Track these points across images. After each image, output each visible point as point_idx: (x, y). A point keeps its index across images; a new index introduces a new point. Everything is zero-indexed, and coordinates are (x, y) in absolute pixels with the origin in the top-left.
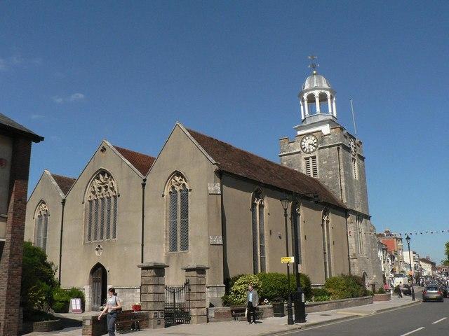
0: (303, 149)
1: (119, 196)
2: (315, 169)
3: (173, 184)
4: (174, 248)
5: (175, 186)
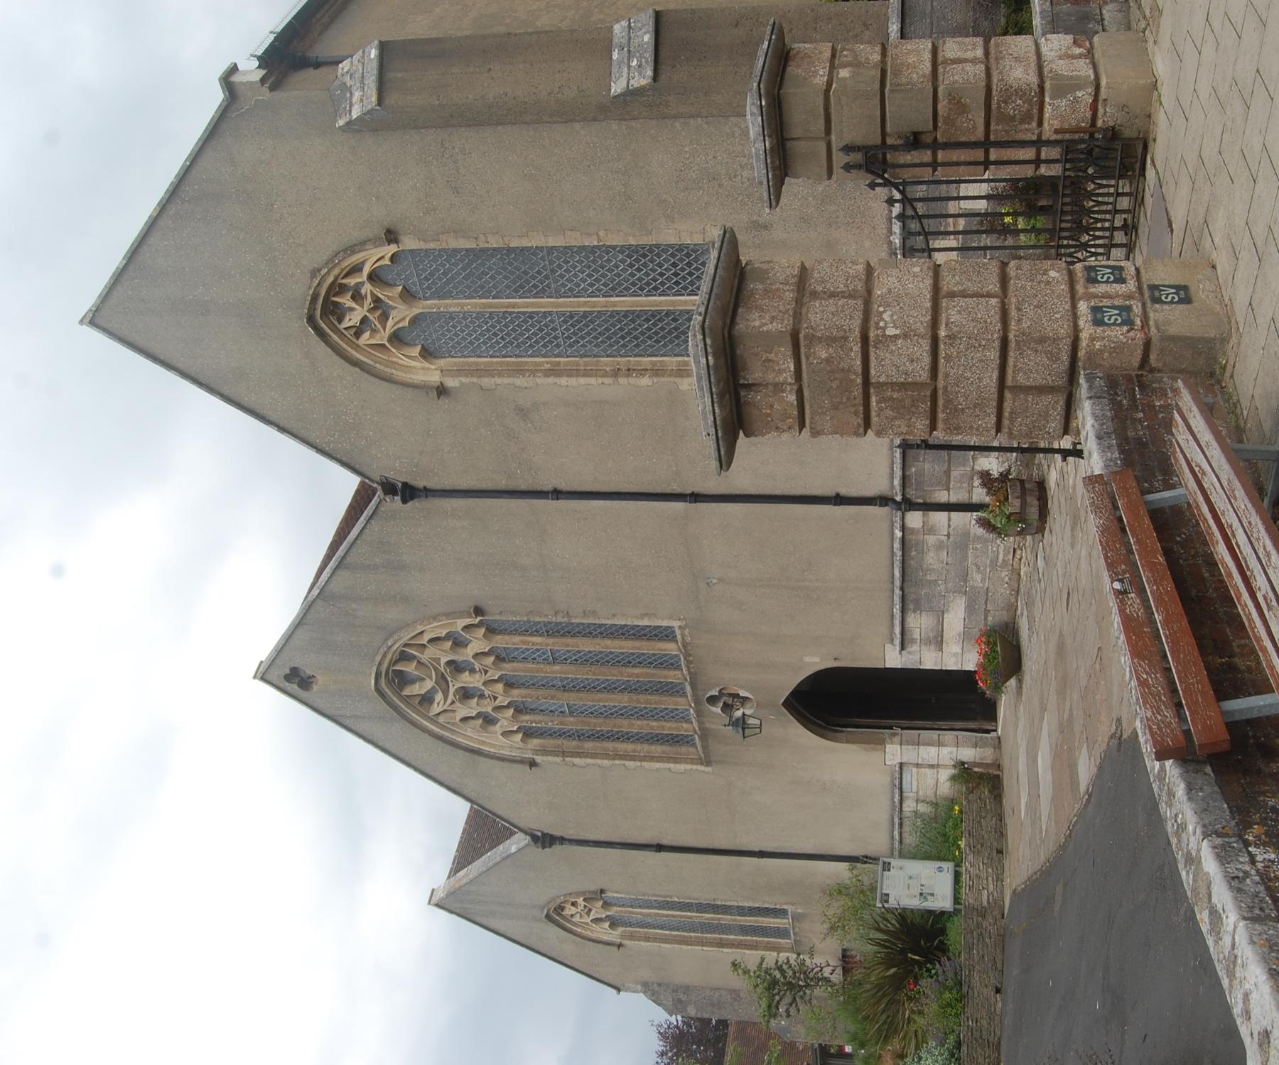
1: (478, 611)
3: (382, 337)
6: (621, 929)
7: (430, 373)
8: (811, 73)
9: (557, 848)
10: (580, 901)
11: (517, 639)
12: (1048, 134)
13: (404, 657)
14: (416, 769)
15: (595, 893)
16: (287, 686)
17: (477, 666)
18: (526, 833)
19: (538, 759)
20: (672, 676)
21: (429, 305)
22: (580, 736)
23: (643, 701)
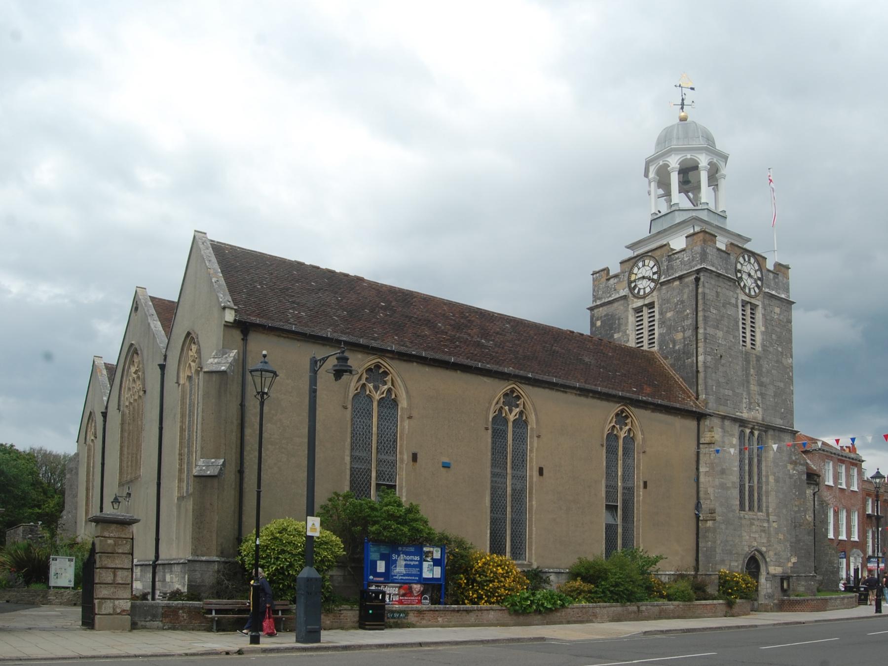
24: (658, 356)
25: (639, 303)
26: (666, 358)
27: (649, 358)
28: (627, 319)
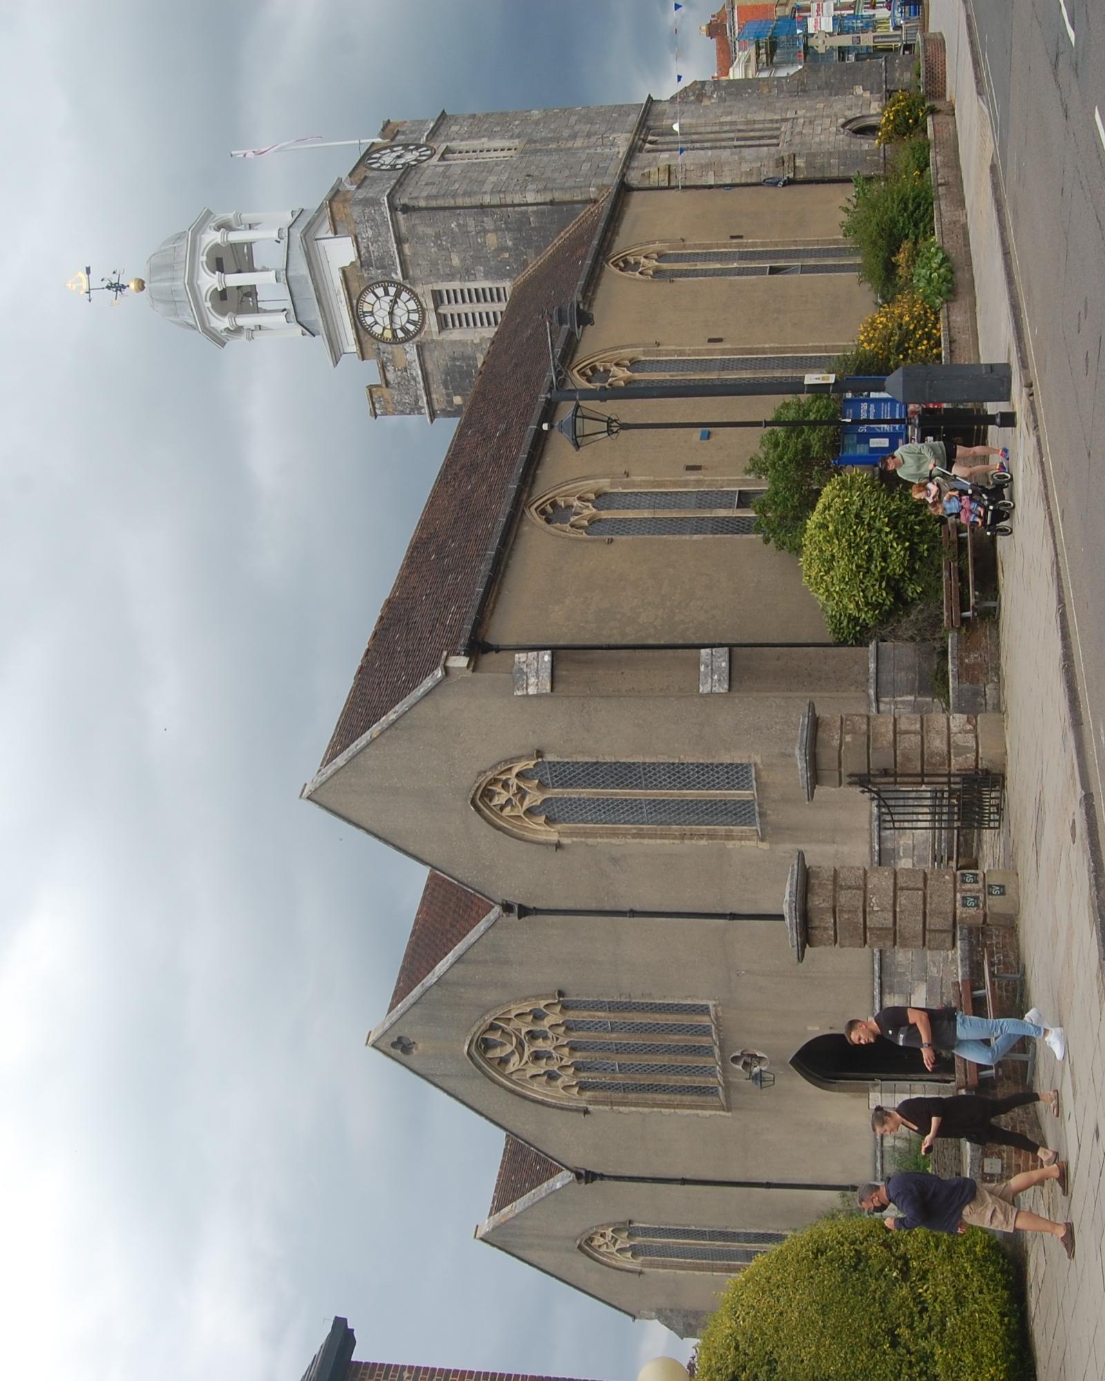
0: (409, 336)
1: (561, 994)
2: (480, 296)
3: (520, 811)
4: (740, 813)
5: (527, 803)
6: (641, 1258)
7: (551, 834)
8: (831, 737)
9: (598, 1183)
10: (609, 1232)
11: (585, 1014)
12: (953, 770)
13: (493, 1027)
14: (487, 1118)
15: (624, 1223)
16: (393, 1051)
17: (550, 1034)
18: (572, 1171)
19: (591, 1108)
20: (704, 1041)
21: (556, 792)
22: (626, 1088)
23: (679, 1060)
24: (520, 279)
25: (432, 318)
26: (525, 264)
27: (518, 302)
28: (454, 343)
